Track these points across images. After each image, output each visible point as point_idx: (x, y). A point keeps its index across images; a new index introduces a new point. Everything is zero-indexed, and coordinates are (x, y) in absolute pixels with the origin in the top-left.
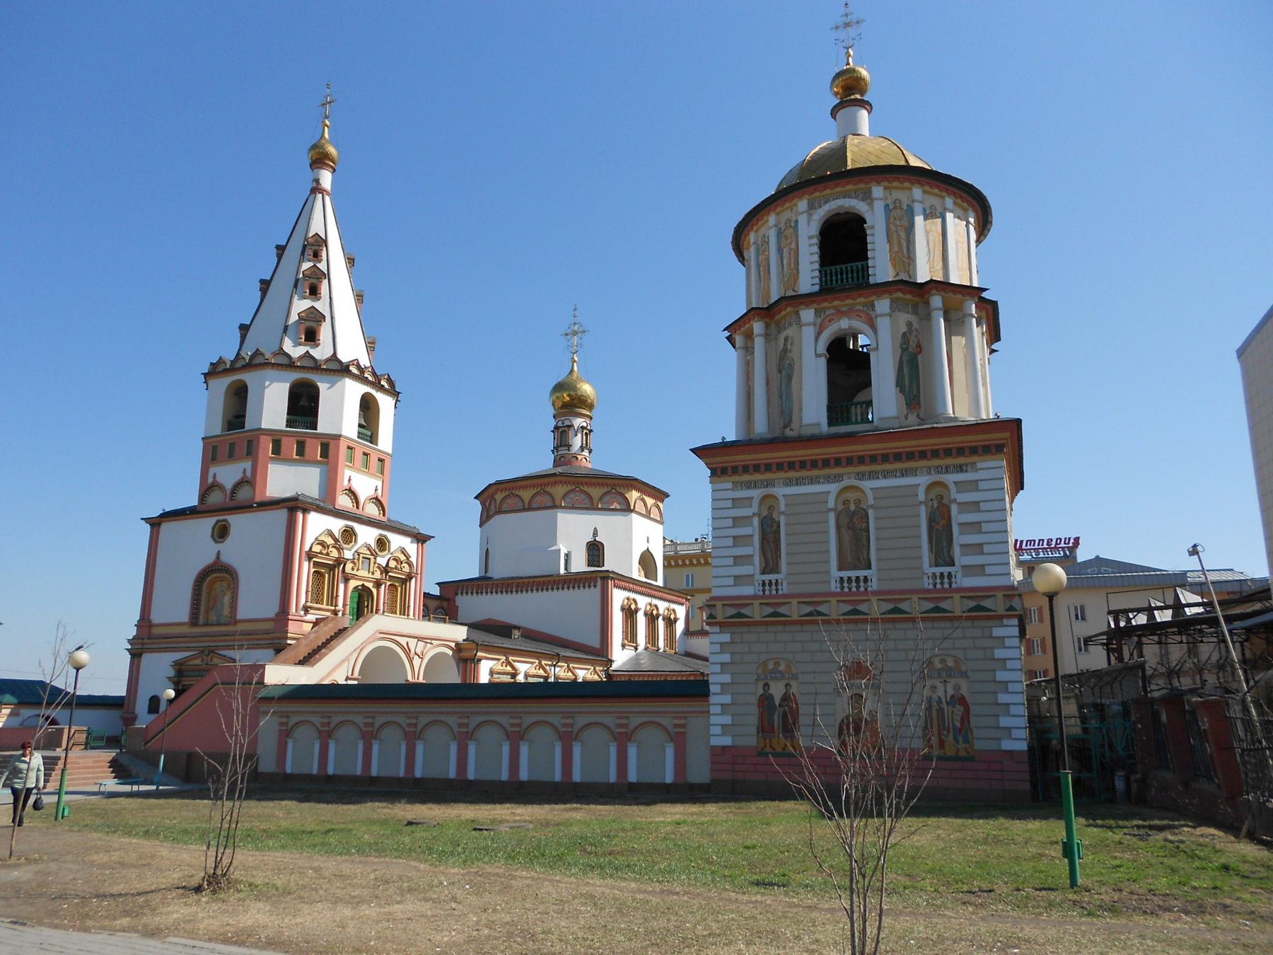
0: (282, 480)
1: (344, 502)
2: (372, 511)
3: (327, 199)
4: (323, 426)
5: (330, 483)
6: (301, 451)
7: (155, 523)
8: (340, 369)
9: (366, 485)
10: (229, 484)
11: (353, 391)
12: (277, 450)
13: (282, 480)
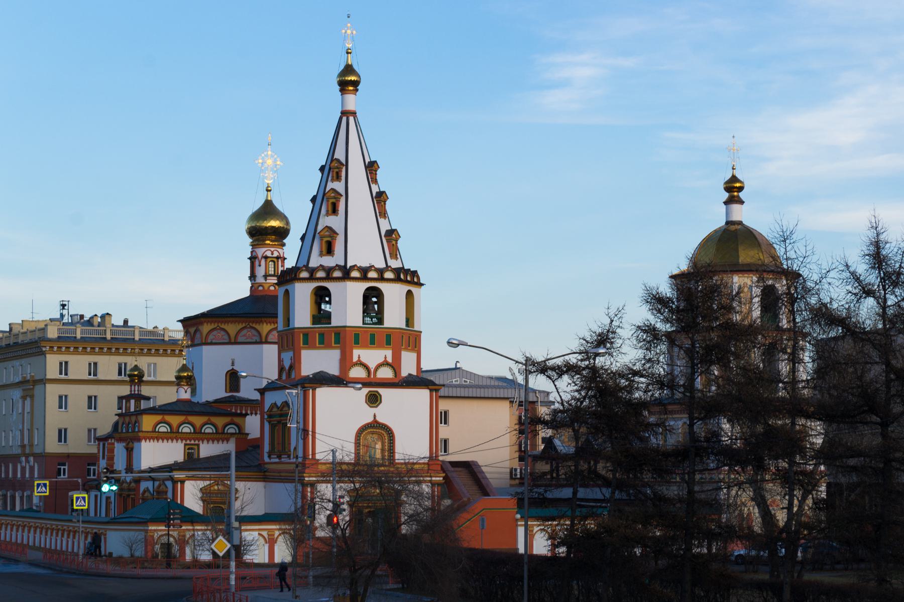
0: (315, 361)
1: (357, 373)
2: (386, 373)
3: (351, 119)
4: (335, 322)
5: (346, 362)
6: (321, 342)
7: (262, 392)
8: (346, 273)
9: (373, 356)
10: (287, 368)
11: (354, 291)
12: (306, 342)
13: (315, 361)
